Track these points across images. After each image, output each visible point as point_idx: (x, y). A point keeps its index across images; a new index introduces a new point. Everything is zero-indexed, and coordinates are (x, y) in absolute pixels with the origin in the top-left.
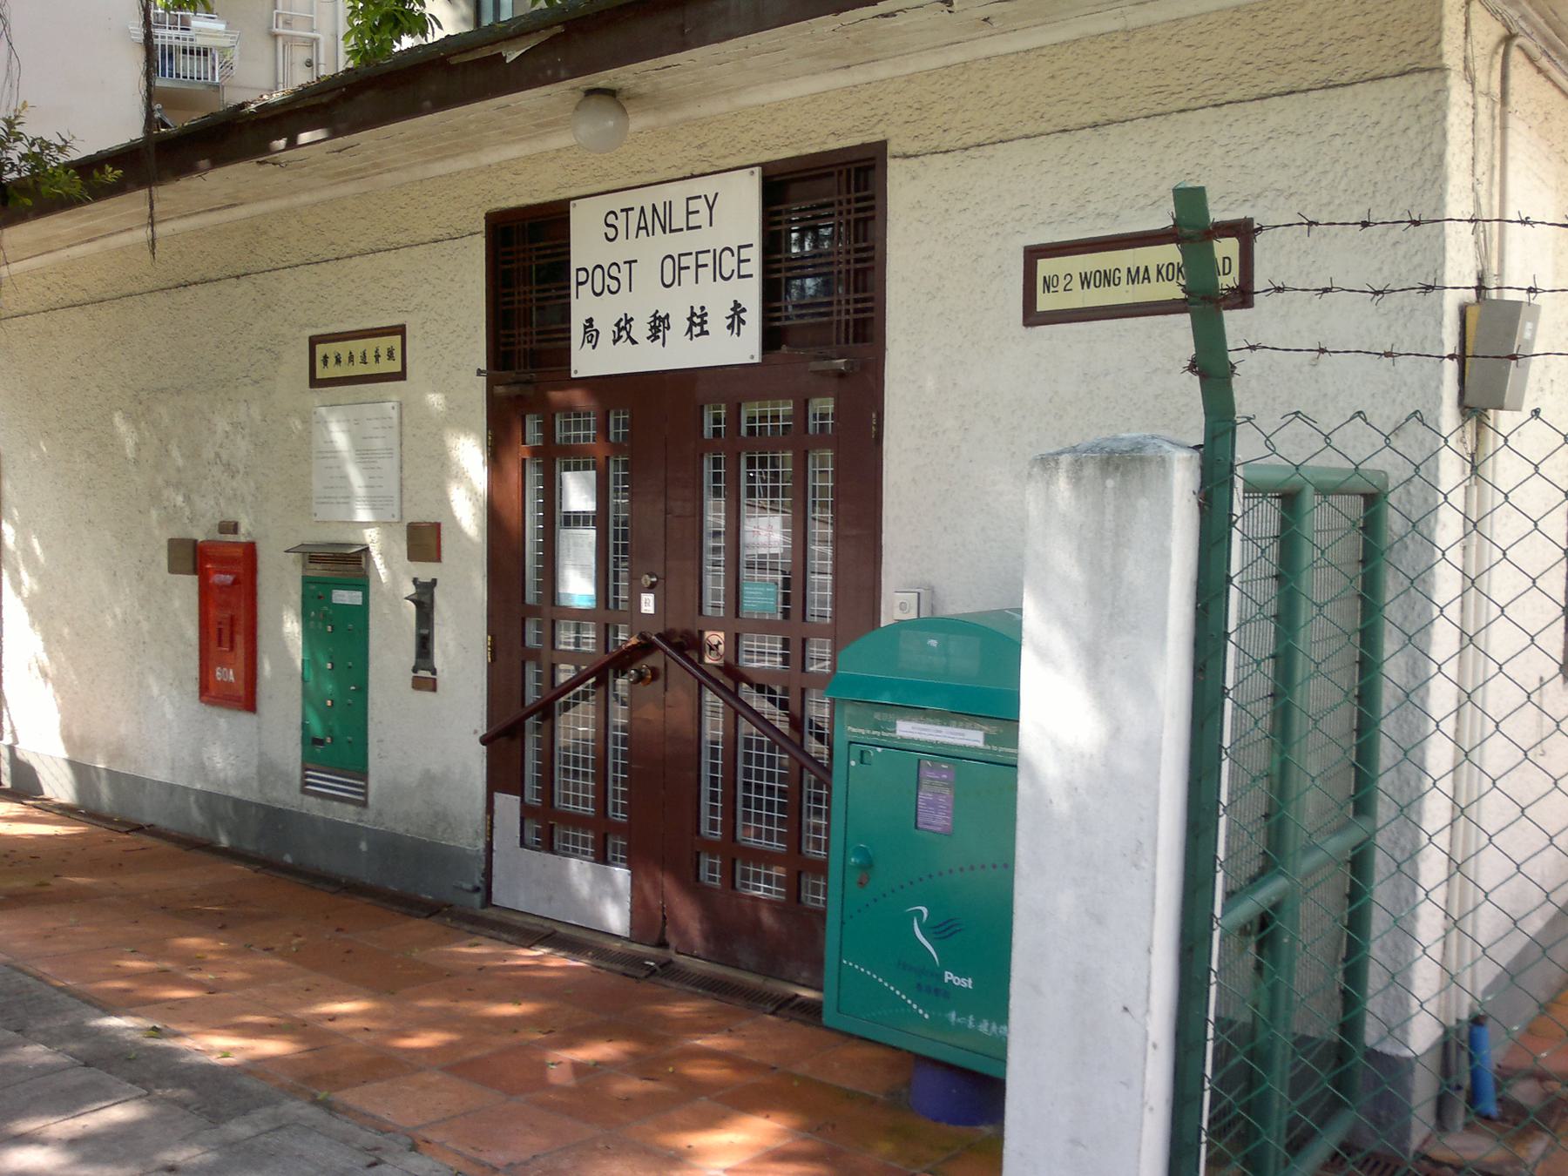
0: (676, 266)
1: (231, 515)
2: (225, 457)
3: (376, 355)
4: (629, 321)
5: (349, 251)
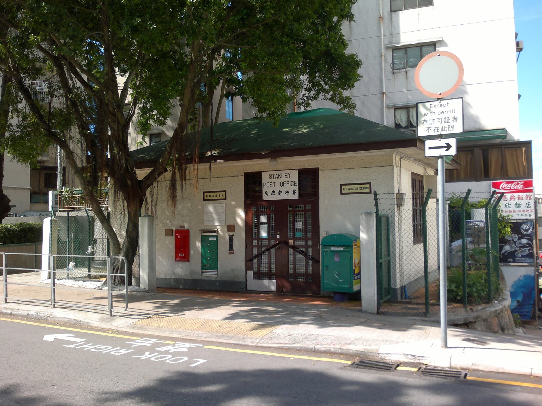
1: (182, 224)
3: (221, 195)
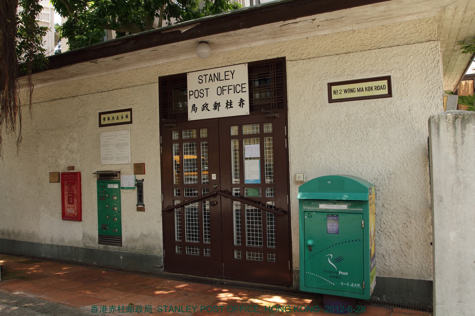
0: (222, 90)
1: (71, 165)
2: (69, 148)
3: (123, 117)
4: (207, 105)
5: (112, 89)
